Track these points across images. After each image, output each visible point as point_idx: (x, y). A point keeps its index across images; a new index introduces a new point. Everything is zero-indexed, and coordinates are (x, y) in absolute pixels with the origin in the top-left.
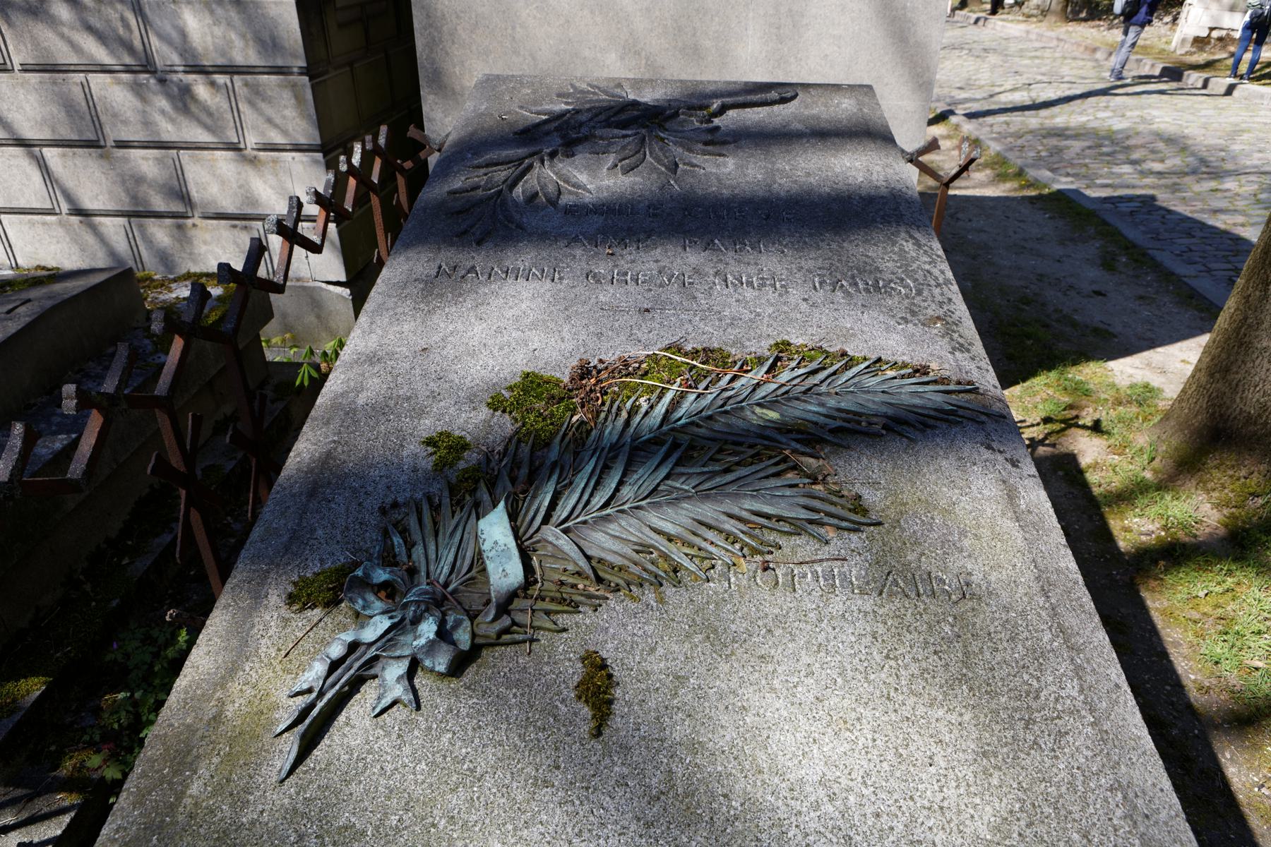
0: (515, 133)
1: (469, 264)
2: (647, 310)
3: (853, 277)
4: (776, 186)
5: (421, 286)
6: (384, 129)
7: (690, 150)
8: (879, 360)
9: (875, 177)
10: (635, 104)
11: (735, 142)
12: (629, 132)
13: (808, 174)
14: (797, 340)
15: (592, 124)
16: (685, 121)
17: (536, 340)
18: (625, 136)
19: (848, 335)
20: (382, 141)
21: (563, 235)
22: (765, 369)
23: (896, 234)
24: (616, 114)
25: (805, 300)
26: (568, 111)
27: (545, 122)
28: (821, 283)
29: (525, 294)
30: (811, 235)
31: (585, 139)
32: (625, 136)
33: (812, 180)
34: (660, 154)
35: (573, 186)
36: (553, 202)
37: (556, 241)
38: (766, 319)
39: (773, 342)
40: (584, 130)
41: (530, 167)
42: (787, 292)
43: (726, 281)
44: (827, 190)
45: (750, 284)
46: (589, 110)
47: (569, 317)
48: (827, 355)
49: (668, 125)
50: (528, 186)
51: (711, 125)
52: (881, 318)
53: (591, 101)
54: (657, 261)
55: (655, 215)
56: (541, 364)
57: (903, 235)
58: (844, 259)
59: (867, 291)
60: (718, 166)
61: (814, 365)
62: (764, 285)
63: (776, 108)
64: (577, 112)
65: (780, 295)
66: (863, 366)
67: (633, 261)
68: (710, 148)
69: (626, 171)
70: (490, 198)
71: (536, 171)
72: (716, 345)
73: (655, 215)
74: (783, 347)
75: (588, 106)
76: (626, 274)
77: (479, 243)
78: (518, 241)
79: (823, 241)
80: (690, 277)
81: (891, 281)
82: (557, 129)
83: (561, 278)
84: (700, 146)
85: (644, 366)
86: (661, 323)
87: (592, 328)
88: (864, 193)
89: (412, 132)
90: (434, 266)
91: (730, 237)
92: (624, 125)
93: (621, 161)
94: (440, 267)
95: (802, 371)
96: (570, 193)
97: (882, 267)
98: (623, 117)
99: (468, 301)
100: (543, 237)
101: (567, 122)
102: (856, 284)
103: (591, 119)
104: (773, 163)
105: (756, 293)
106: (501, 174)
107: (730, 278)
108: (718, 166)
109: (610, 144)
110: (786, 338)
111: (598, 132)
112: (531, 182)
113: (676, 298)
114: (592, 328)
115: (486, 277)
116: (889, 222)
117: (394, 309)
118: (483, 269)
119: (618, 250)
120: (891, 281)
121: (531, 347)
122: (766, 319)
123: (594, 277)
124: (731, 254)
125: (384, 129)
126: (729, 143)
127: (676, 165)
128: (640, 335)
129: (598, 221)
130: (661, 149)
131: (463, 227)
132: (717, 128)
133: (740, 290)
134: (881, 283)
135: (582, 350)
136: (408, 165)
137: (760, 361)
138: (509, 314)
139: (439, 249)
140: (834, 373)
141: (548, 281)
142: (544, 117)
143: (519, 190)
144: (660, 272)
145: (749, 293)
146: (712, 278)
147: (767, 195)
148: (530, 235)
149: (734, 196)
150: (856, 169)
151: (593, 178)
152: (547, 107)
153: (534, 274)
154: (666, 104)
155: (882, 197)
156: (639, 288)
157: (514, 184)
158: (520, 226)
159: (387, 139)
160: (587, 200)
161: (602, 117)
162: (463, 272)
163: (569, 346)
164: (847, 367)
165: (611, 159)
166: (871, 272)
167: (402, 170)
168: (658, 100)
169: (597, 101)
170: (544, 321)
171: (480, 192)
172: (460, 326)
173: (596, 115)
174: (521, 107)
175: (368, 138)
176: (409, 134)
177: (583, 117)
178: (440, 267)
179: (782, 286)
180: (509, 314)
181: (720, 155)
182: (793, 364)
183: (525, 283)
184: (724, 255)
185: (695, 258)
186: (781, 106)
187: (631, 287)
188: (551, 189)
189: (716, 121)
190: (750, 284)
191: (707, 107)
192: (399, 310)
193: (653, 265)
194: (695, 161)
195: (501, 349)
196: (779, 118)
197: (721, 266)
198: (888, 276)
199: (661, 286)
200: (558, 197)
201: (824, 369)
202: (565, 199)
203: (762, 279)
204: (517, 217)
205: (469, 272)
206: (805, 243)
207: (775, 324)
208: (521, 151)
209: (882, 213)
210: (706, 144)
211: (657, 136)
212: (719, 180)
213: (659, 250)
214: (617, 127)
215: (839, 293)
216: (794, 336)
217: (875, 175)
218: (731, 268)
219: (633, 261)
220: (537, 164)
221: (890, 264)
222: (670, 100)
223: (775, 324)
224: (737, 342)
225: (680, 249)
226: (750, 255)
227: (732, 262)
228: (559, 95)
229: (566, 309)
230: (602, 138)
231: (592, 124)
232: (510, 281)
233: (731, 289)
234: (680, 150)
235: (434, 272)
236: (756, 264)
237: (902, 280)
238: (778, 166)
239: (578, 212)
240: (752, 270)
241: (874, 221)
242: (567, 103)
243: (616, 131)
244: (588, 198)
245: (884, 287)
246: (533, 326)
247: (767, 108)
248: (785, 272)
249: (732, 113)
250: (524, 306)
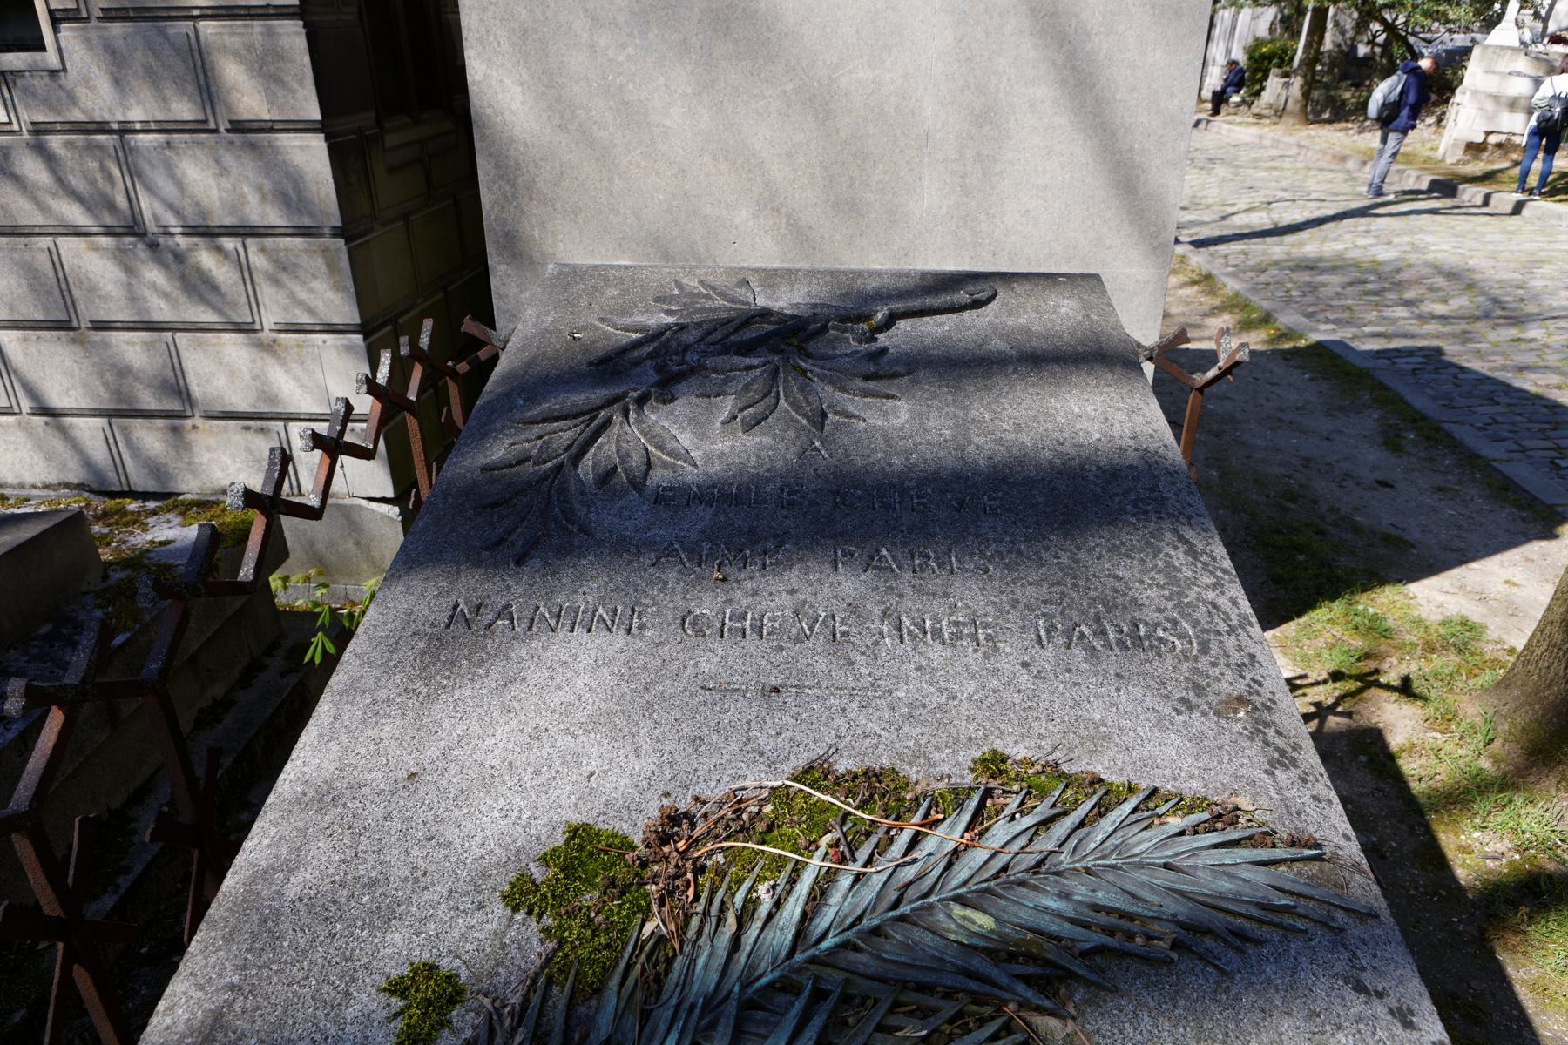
0: (590, 364)
2: (776, 690)
3: (1098, 619)
4: (971, 449)
5: (422, 645)
6: (428, 324)
7: (844, 390)
8: (1154, 791)
10: (765, 314)
11: (909, 373)
12: (755, 361)
14: (1018, 751)
15: (702, 347)
16: (836, 338)
17: (595, 752)
18: (749, 368)
20: (424, 341)
21: (649, 544)
22: (966, 817)
23: (1157, 534)
24: (736, 330)
25: (1025, 665)
26: (668, 327)
27: (637, 344)
28: (1048, 631)
30: (1028, 539)
31: (692, 371)
32: (749, 368)
33: (1024, 437)
34: (800, 397)
35: (670, 455)
36: (637, 484)
37: (639, 554)
38: (965, 705)
39: (978, 755)
40: (692, 356)
41: (608, 422)
42: (996, 650)
43: (899, 629)
45: (937, 633)
46: (699, 325)
47: (650, 705)
48: (1069, 781)
49: (812, 346)
50: (602, 455)
51: (874, 346)
53: (702, 310)
54: (792, 592)
55: (791, 504)
56: (600, 807)
57: (1168, 536)
58: (1082, 583)
59: (1120, 643)
60: (885, 414)
61: (1043, 810)
62: (957, 636)
63: (966, 314)
64: (682, 328)
65: (986, 656)
66: (1128, 807)
68: (872, 385)
69: (749, 427)
70: (544, 478)
71: (615, 429)
72: (886, 762)
74: (994, 764)
75: (697, 318)
76: (743, 617)
77: (519, 563)
78: (581, 556)
79: (1047, 549)
80: (843, 622)
81: (1158, 624)
82: (651, 356)
83: (641, 628)
84: (859, 383)
85: (768, 809)
86: (796, 716)
87: (686, 728)
89: (469, 326)
91: (905, 544)
92: (746, 349)
93: (741, 410)
94: (455, 607)
95: (1028, 821)
96: (665, 465)
97: (1142, 599)
98: (749, 334)
99: (494, 675)
100: (621, 547)
101: (666, 345)
103: (702, 339)
104: (966, 408)
105: (948, 653)
106: (565, 435)
107: (906, 622)
108: (885, 414)
109: (725, 382)
110: (998, 745)
111: (710, 362)
112: (606, 449)
113: (822, 664)
114: (686, 728)
116: (1146, 513)
120: (1158, 624)
122: (965, 705)
123: (693, 624)
124: (907, 576)
125: (428, 324)
126: (900, 375)
127: (824, 415)
128: (762, 741)
129: (703, 515)
130: (801, 389)
131: (499, 531)
132: (884, 351)
135: (668, 773)
136: (463, 367)
137: (958, 796)
139: (458, 572)
140: (1081, 824)
141: (622, 632)
142: (635, 336)
143: (588, 460)
146: (877, 622)
147: (959, 464)
148: (599, 544)
149: (910, 468)
150: (1090, 419)
151: (699, 439)
152: (640, 319)
154: (810, 312)
155: (1131, 467)
157: (582, 452)
158: (585, 530)
159: (432, 337)
160: (689, 479)
161: (717, 335)
162: (490, 617)
163: (645, 765)
164: (1102, 810)
165: (727, 405)
166: (1125, 609)
167: (454, 374)
168: (797, 305)
169: (711, 309)
170: (610, 714)
171: (530, 467)
172: (475, 728)
173: (709, 333)
174: (602, 320)
175: (404, 340)
176: (464, 328)
177: (689, 337)
178: (455, 607)
179: (989, 638)
180: (555, 699)
181: (888, 397)
182: (1013, 803)
183: (585, 637)
185: (850, 584)
186: (975, 313)
187: (751, 643)
188: (636, 460)
189: (882, 339)
191: (868, 317)
192: (382, 694)
193: (786, 600)
194: (851, 408)
195: (537, 773)
196: (972, 332)
197: (892, 600)
199: (798, 640)
201: (1066, 813)
202: (658, 477)
203: (956, 624)
204: (581, 511)
205: (499, 617)
206: (1020, 553)
207: (979, 716)
208: (600, 394)
210: (867, 378)
211: (797, 367)
212: (887, 440)
213: (795, 571)
214: (738, 353)
217: (1117, 426)
219: (755, 593)
220: (617, 419)
221: (1152, 593)
222: (815, 306)
223: (979, 716)
225: (827, 568)
226: (935, 584)
227: (909, 591)
228: (657, 300)
229: (646, 689)
230: (715, 371)
231: (702, 347)
232: (562, 633)
234: (829, 389)
236: (946, 595)
237: (1175, 623)
238: (974, 413)
239: (677, 499)
240: (940, 607)
241: (1123, 510)
242: (669, 313)
243: (737, 360)
244: (690, 474)
245: (1149, 636)
247: (953, 316)
248: (991, 609)
249: (903, 325)
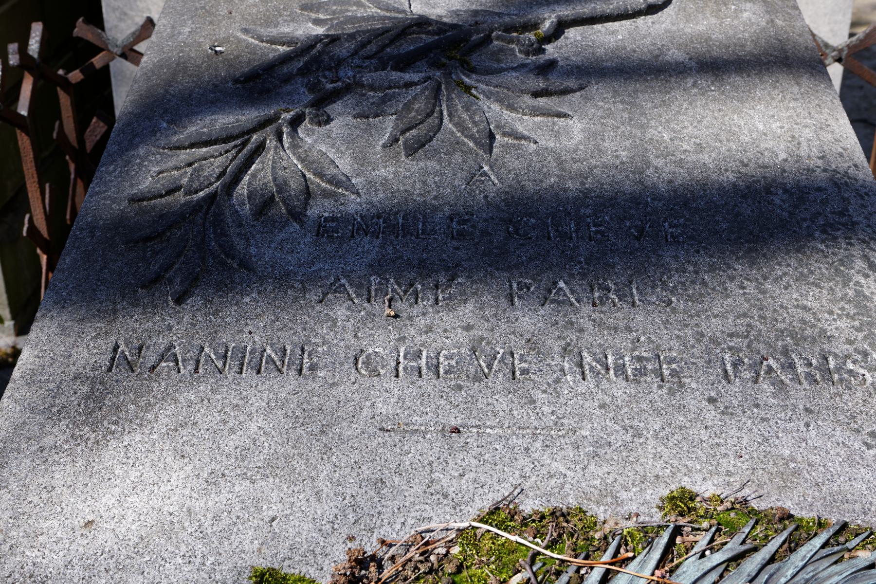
0: (236, 81)
1: (162, 342)
2: (456, 430)
3: (786, 352)
4: (650, 172)
5: (85, 389)
6: (37, 30)
7: (512, 108)
8: (844, 526)
9: (804, 151)
10: (422, 22)
11: (581, 88)
12: (415, 77)
13: (700, 148)
14: (706, 488)
15: (357, 61)
16: (501, 50)
17: (274, 496)
18: (409, 85)
19: (789, 475)
20: (34, 46)
21: (315, 278)
22: (656, 555)
23: (846, 262)
24: (392, 41)
25: (712, 401)
26: (318, 39)
27: (285, 59)
28: (734, 365)
29: (257, 403)
30: (712, 269)
31: (347, 89)
32: (409, 85)
33: (706, 158)
34: (465, 116)
35: (330, 182)
36: (297, 215)
37: (304, 290)
38: (651, 443)
39: (666, 493)
40: (347, 74)
41: (260, 148)
42: (681, 385)
43: (581, 365)
44: (732, 177)
45: (620, 369)
46: (351, 36)
47: (328, 448)
48: (758, 517)
49: (474, 59)
50: (258, 184)
51: (542, 58)
52: (839, 436)
53: (353, 20)
54: (468, 328)
55: (461, 235)
56: (284, 552)
57: (859, 264)
58: (769, 314)
59: (810, 377)
60: (557, 134)
61: (734, 546)
62: (641, 372)
63: (641, 21)
64: (334, 40)
65: (671, 392)
66: (818, 542)
67: (429, 330)
68: (542, 101)
69: (412, 150)
70: (196, 208)
71: (270, 154)
72: (572, 502)
73: (461, 235)
74: (682, 502)
75: (349, 29)
76: (418, 355)
77: (180, 300)
78: (245, 293)
79: (732, 279)
80: (522, 359)
81: (848, 357)
83: (313, 368)
84: (528, 100)
85: (456, 550)
86: (479, 457)
87: (366, 471)
88: (789, 181)
89: (82, 30)
90: (106, 345)
91: (584, 275)
92: (404, 63)
93: (403, 132)
94: (116, 348)
95: (718, 557)
96: (326, 194)
97: (831, 330)
98: (407, 46)
99: (163, 420)
100: (289, 282)
101: (317, 60)
102: (792, 366)
103: (355, 53)
104: (643, 127)
105: (632, 389)
106: (216, 162)
107: (588, 358)
108: (557, 134)
109: (384, 101)
110: (687, 483)
111: (367, 78)
112: (261, 173)
113: (502, 403)
114: (366, 471)
115: (190, 367)
116: (835, 239)
117: (38, 438)
118: (185, 351)
119: (401, 306)
120: (848, 357)
121: (267, 514)
122: (651, 443)
123: (367, 363)
124: (587, 309)
125: (37, 30)
126: (573, 91)
127: (492, 137)
128: (445, 482)
129: (370, 246)
130: (467, 108)
131: (155, 267)
132: (552, 64)
133: (605, 384)
134: (832, 363)
135: (351, 517)
136: (75, 76)
137: (648, 534)
138: (230, 443)
139: (115, 311)
140: (772, 560)
141: (293, 373)
142: (282, 49)
143: (243, 189)
144: (474, 350)
145: (620, 390)
146: (558, 359)
147: (637, 189)
148: (262, 279)
149: (586, 193)
150: (776, 137)
152: (286, 29)
153: (270, 360)
154: (471, 20)
155: (819, 189)
156: (441, 384)
157: (236, 179)
158: (245, 265)
159: (43, 43)
160: (352, 208)
161: (372, 48)
162: (154, 358)
163: (328, 509)
164: (792, 545)
165: (388, 125)
166: (814, 341)
167: (66, 84)
168: (456, 13)
169: (363, 19)
170: (287, 458)
171: (180, 197)
172: (149, 475)
173: (363, 45)
174: (246, 31)
175: (13, 47)
176: (76, 32)
177: (342, 50)
178: (116, 348)
179: (674, 373)
180: (230, 443)
181: (560, 115)
182: (703, 540)
183: (255, 379)
184: (576, 311)
185: (529, 319)
186: (650, 19)
187: (428, 382)
188: (294, 185)
189: (550, 49)
190: (620, 369)
191: (535, 26)
192: (49, 441)
193: (461, 336)
194: (520, 128)
195: (216, 518)
196: (648, 41)
197: (572, 335)
198: (842, 348)
199: (476, 379)
200: (306, 204)
201: (755, 549)
202: (318, 209)
203: (640, 359)
204: (240, 245)
205: (162, 358)
206: (704, 283)
207: (666, 453)
208: (249, 116)
209: (821, 221)
210: (536, 94)
211: (460, 83)
212: (560, 163)
213: (470, 306)
214: (396, 68)
215: (765, 386)
216: (698, 477)
217: (804, 145)
218: (589, 338)
219: (429, 330)
220: (271, 143)
221: (842, 324)
222: (476, 13)
223: (666, 453)
224: (607, 493)
225: (504, 303)
226: (617, 316)
227: (589, 326)
228: (304, 7)
229: (323, 432)
230: (372, 88)
231: (357, 61)
232: (231, 374)
233: (591, 382)
234: (496, 107)
235: (105, 361)
236: (628, 329)
237: (865, 354)
238: (651, 132)
239: (339, 231)
240: (622, 341)
241: (810, 236)
242: (317, 22)
243: (395, 75)
244: (353, 204)
245: (838, 369)
246: (270, 468)
247: (626, 23)
248: (675, 344)
249: (573, 33)
250: (253, 427)
